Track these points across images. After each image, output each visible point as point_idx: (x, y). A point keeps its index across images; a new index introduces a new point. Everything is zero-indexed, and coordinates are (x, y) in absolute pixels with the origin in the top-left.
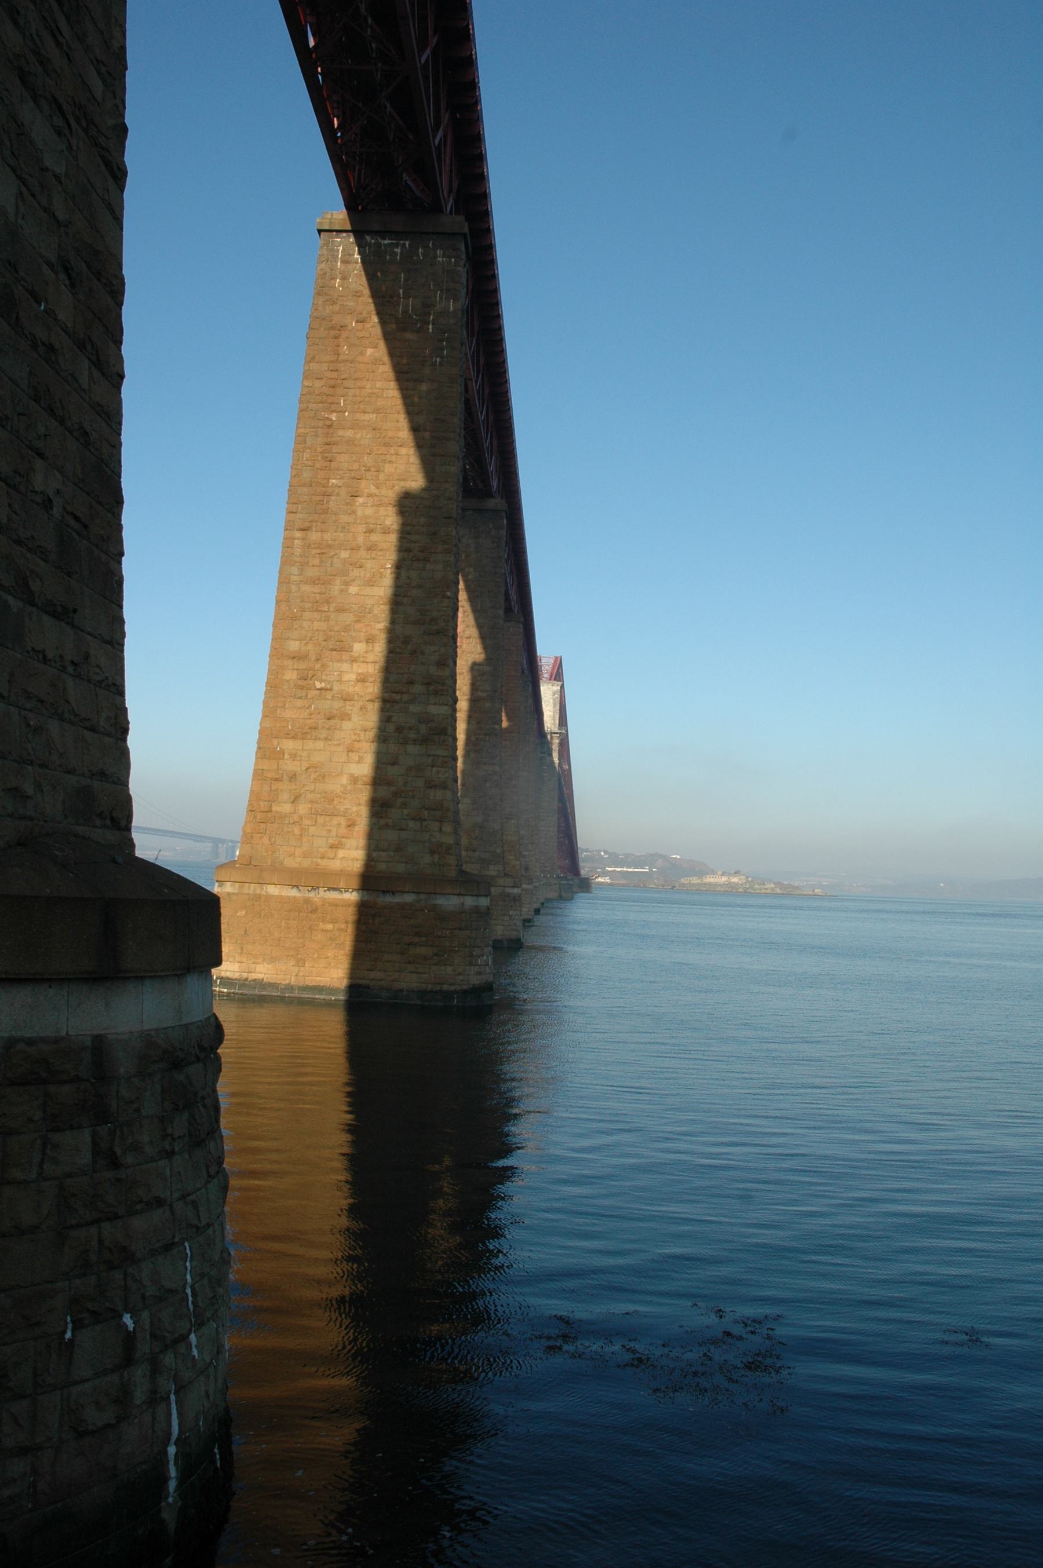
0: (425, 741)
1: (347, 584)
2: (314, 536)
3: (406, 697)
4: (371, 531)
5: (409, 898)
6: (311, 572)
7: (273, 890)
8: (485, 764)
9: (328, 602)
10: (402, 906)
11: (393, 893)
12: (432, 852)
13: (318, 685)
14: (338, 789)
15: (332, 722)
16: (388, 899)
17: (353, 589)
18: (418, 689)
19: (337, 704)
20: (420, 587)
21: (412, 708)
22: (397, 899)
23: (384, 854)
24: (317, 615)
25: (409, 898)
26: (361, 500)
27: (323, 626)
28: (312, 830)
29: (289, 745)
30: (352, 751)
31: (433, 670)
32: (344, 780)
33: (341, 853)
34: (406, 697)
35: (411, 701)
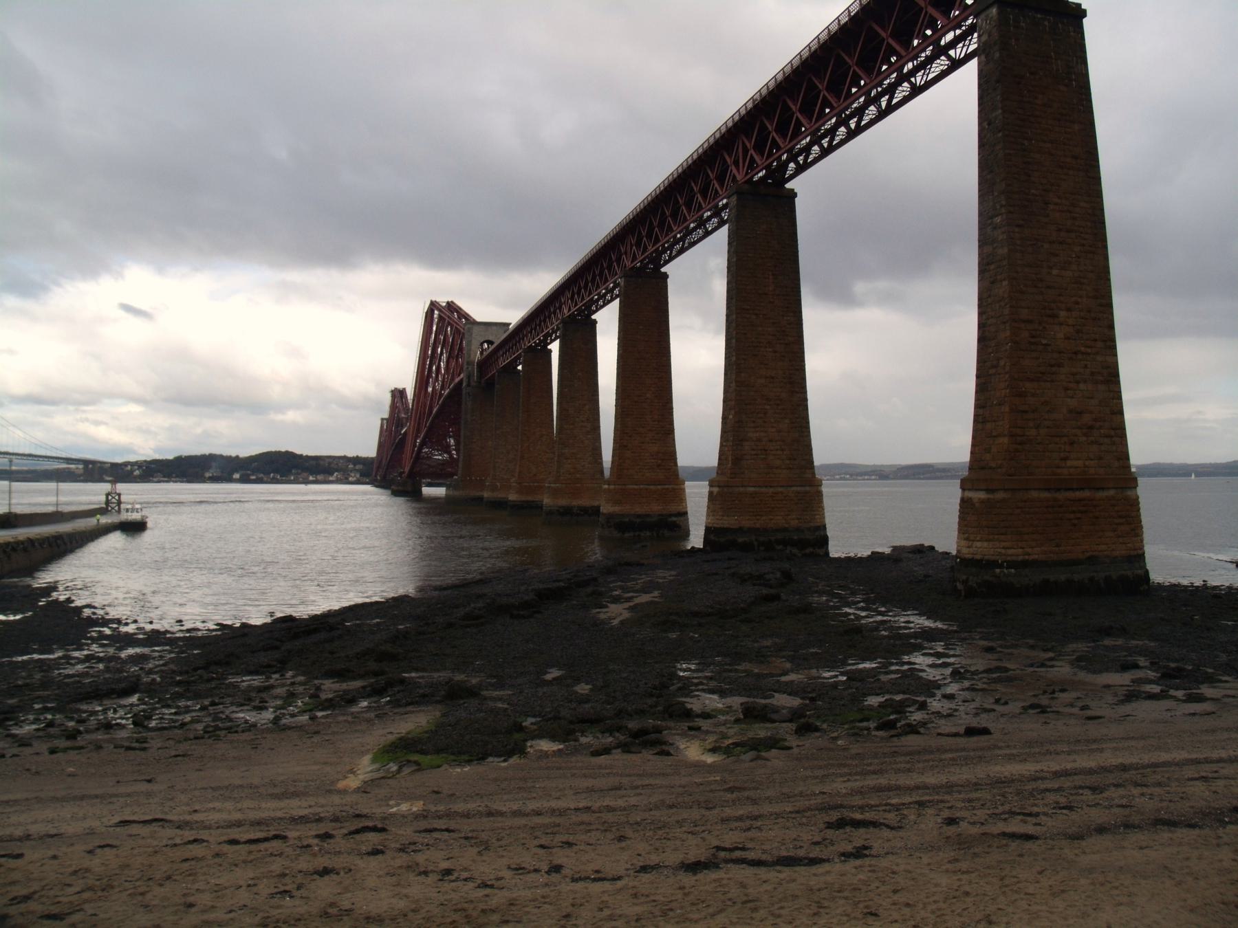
1: (1051, 268)
4: (1060, 230)
5: (1112, 492)
7: (1035, 494)
8: (797, 393)
11: (1103, 489)
13: (1044, 342)
15: (1054, 369)
17: (1055, 272)
18: (1099, 344)
20: (1092, 272)
21: (1099, 358)
23: (1092, 462)
26: (1051, 207)
30: (1068, 389)
33: (1069, 463)
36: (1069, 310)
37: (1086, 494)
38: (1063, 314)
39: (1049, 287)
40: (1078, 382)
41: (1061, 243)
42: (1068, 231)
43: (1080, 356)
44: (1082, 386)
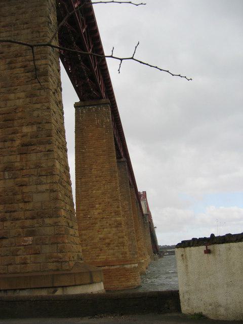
0: (117, 227)
2: (83, 180)
3: (110, 216)
4: (96, 177)
5: (118, 266)
6: (83, 189)
9: (88, 196)
10: (116, 269)
11: (114, 266)
12: (122, 254)
13: (89, 216)
14: (97, 241)
16: (113, 267)
17: (94, 192)
18: (113, 214)
19: (94, 220)
20: (110, 189)
21: (113, 219)
22: (115, 267)
24: (86, 199)
25: (118, 266)
27: (88, 202)
28: (92, 252)
29: (83, 232)
31: (117, 209)
32: (98, 239)
33: (100, 257)
34: (110, 216)
35: (112, 217)
36: (100, 204)
37: (106, 268)
38: (97, 206)
39: (92, 197)
40: (104, 229)
41: (96, 182)
42: (100, 177)
43: (104, 219)
44: (105, 230)
